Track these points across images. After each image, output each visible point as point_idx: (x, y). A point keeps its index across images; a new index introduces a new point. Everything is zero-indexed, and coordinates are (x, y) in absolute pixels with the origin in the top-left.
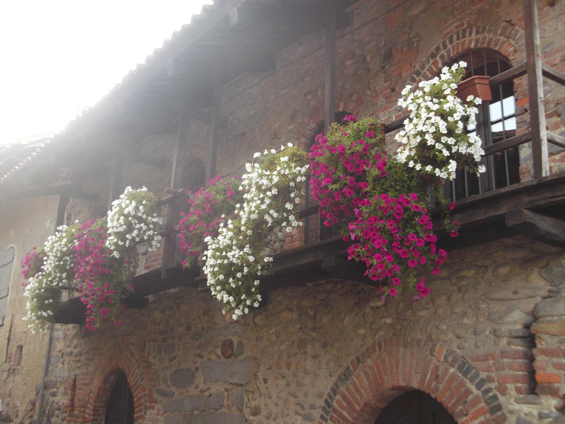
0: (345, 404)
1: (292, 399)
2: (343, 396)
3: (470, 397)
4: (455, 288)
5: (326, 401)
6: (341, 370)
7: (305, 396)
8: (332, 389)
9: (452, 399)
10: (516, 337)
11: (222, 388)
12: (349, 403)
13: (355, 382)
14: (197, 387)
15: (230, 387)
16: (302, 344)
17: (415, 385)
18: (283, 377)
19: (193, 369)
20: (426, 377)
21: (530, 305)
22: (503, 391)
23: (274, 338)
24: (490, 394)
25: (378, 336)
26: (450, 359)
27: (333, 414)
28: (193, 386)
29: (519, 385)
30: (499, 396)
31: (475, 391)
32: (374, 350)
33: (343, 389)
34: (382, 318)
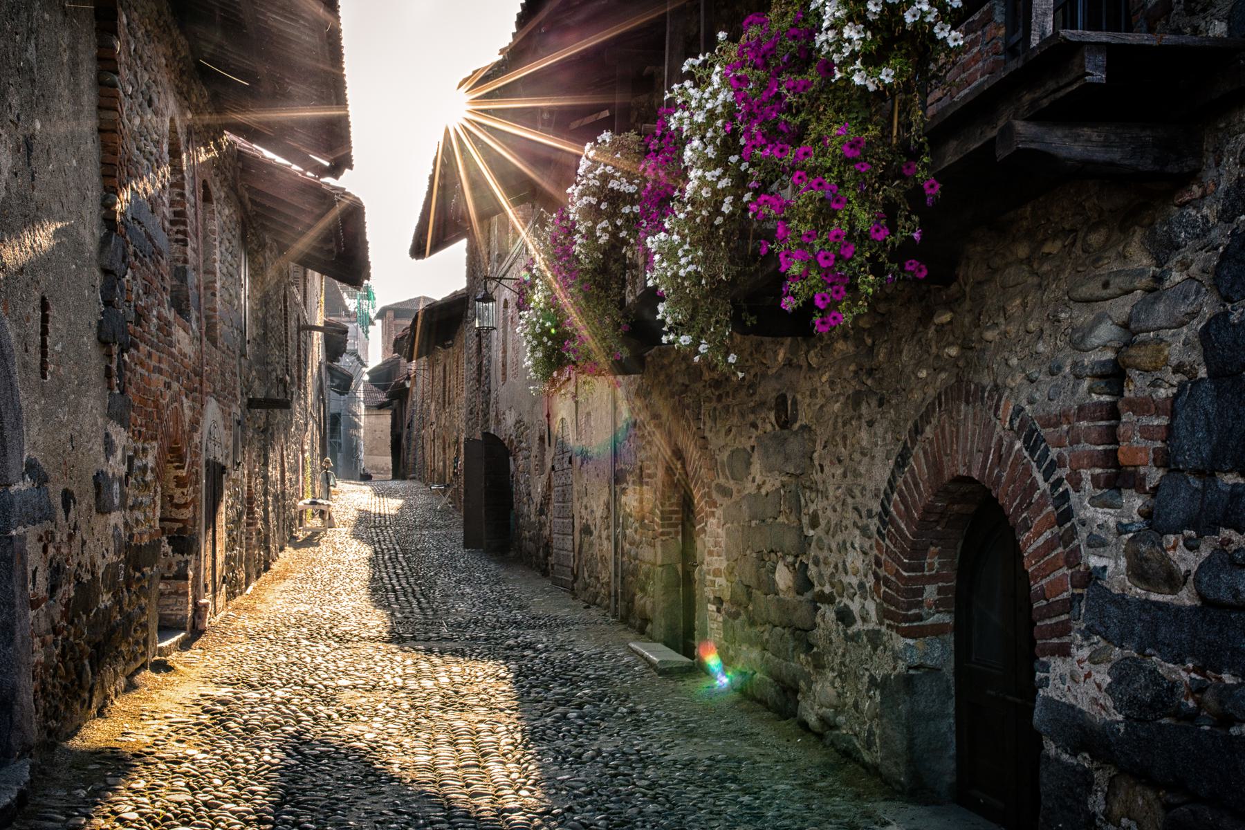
0: (902, 507)
1: (849, 500)
2: (901, 494)
3: (1036, 496)
4: (1035, 280)
5: (882, 504)
6: (899, 448)
7: (863, 495)
8: (889, 482)
9: (1015, 500)
10: (1101, 377)
11: (778, 484)
12: (906, 507)
13: (914, 470)
14: (754, 481)
15: (785, 479)
16: (856, 400)
17: (975, 474)
18: (840, 461)
19: (749, 449)
20: (987, 458)
21: (1122, 308)
22: (1077, 484)
23: (828, 391)
24: (1061, 490)
25: (938, 383)
26: (1016, 424)
27: (890, 527)
28: (750, 478)
29: (1098, 471)
30: (1071, 492)
31: (1043, 485)
32: (934, 411)
33: (900, 481)
34: (945, 347)
